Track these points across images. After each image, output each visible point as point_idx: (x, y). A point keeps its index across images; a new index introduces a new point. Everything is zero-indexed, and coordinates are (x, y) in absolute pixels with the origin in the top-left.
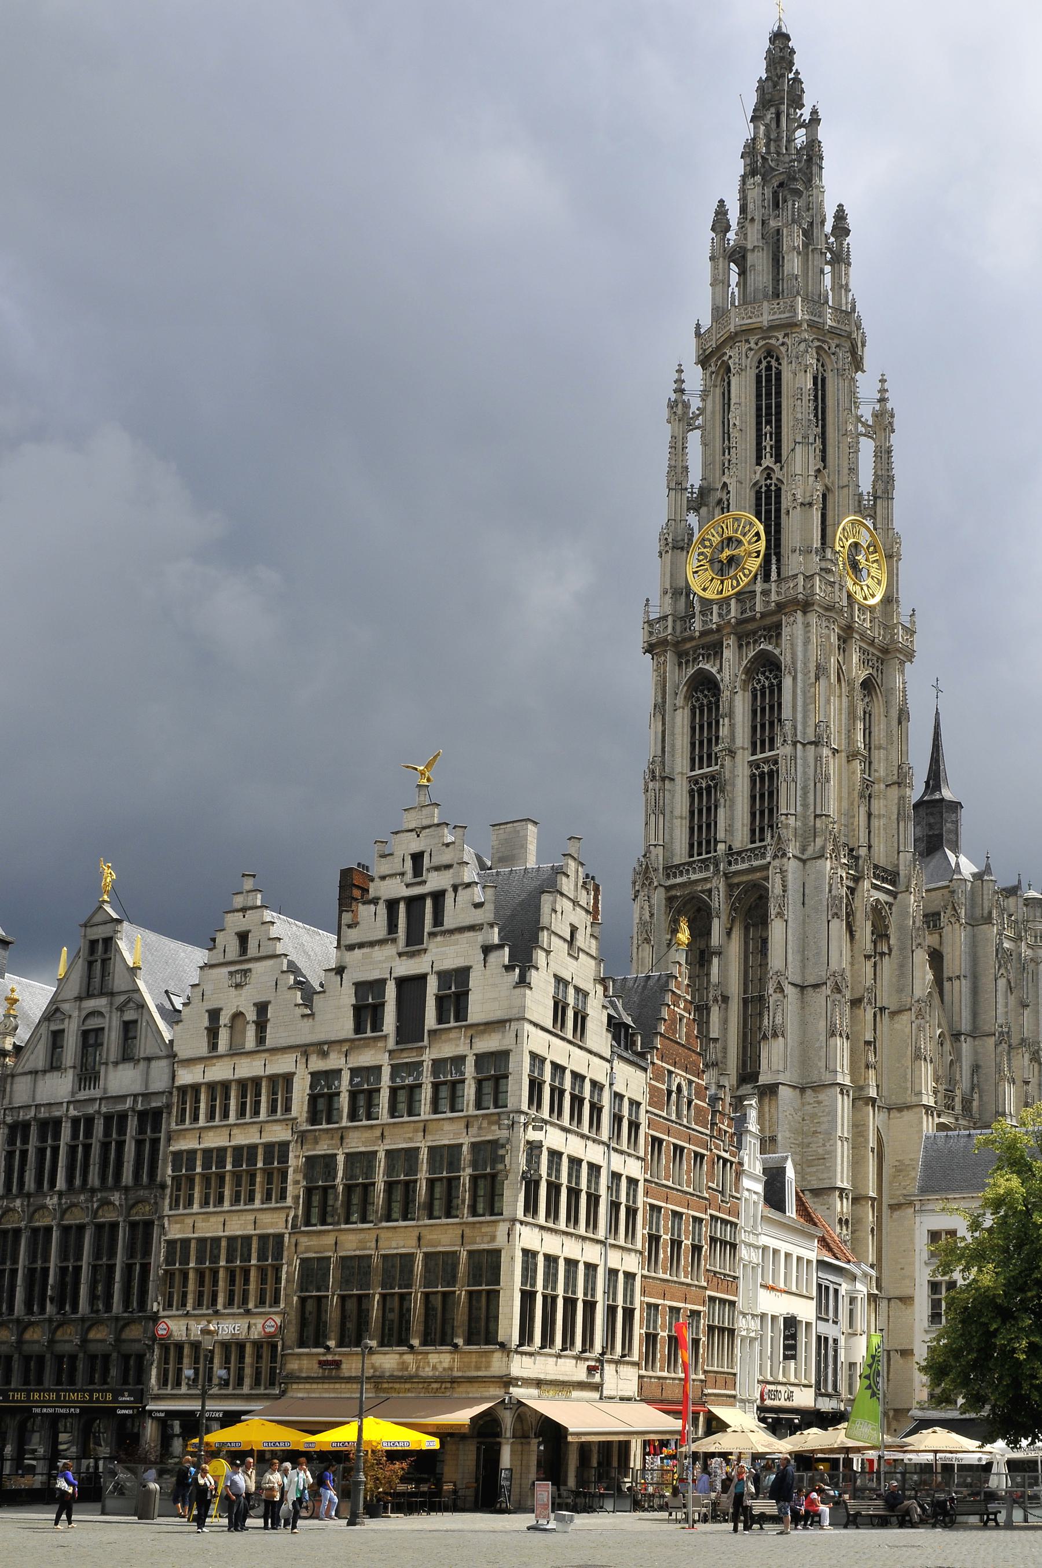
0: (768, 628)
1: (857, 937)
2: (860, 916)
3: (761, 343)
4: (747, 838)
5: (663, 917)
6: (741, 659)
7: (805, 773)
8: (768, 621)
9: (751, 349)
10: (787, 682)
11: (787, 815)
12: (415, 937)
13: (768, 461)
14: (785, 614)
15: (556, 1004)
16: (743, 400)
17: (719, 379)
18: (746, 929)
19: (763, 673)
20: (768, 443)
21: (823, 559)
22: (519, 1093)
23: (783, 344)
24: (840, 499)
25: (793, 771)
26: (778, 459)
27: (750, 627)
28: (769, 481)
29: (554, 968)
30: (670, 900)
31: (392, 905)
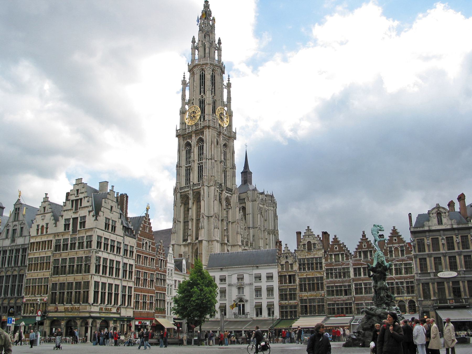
2: (223, 199)
3: (201, 68)
4: (197, 181)
5: (179, 200)
6: (196, 139)
8: (201, 131)
9: (198, 69)
10: (205, 144)
12: (76, 209)
13: (202, 94)
15: (106, 224)
18: (197, 202)
19: (201, 143)
21: (213, 116)
22: (94, 245)
23: (205, 68)
24: (218, 103)
26: (204, 94)
27: (198, 132)
29: (105, 216)
30: (181, 195)
31: (72, 201)
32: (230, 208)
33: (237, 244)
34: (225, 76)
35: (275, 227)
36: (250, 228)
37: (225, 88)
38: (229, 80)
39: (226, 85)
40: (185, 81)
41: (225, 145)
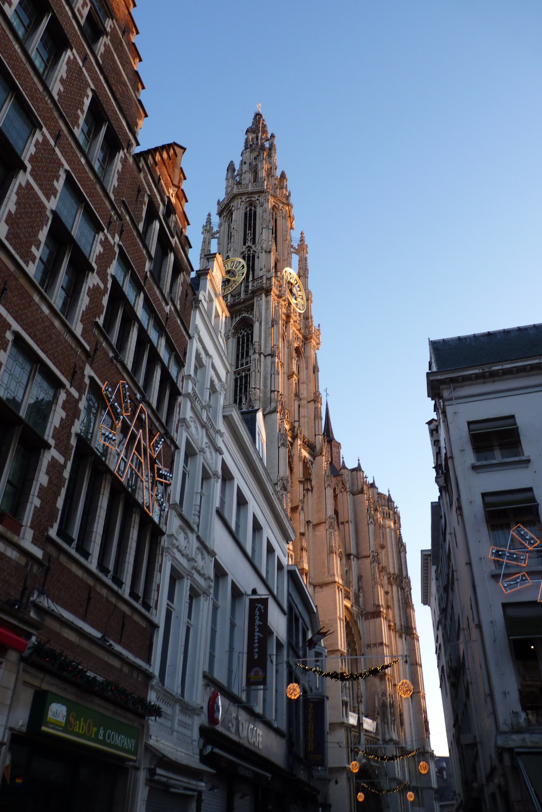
0: (247, 307)
1: (294, 470)
3: (247, 200)
6: (232, 322)
7: (265, 370)
11: (255, 388)
13: (249, 244)
14: (256, 296)
16: (238, 220)
17: (228, 218)
19: (244, 329)
20: (249, 238)
23: (257, 200)
25: (259, 367)
26: (254, 243)
28: (249, 253)
32: (310, 488)
33: (330, 579)
34: (295, 236)
35: (400, 570)
36: (352, 557)
37: (294, 253)
38: (302, 240)
39: (297, 248)
40: (211, 228)
41: (297, 350)
